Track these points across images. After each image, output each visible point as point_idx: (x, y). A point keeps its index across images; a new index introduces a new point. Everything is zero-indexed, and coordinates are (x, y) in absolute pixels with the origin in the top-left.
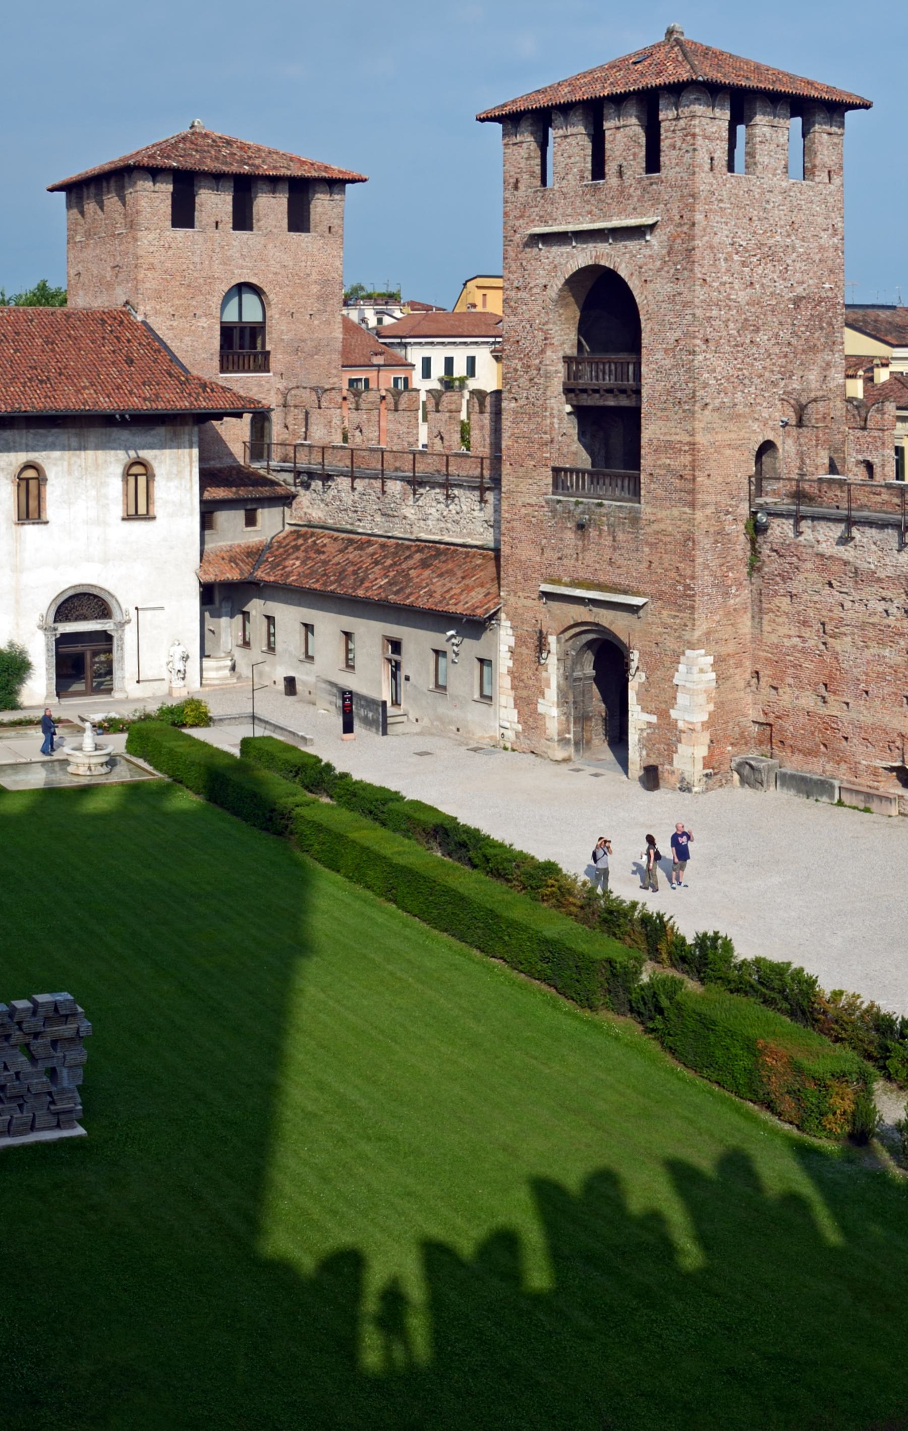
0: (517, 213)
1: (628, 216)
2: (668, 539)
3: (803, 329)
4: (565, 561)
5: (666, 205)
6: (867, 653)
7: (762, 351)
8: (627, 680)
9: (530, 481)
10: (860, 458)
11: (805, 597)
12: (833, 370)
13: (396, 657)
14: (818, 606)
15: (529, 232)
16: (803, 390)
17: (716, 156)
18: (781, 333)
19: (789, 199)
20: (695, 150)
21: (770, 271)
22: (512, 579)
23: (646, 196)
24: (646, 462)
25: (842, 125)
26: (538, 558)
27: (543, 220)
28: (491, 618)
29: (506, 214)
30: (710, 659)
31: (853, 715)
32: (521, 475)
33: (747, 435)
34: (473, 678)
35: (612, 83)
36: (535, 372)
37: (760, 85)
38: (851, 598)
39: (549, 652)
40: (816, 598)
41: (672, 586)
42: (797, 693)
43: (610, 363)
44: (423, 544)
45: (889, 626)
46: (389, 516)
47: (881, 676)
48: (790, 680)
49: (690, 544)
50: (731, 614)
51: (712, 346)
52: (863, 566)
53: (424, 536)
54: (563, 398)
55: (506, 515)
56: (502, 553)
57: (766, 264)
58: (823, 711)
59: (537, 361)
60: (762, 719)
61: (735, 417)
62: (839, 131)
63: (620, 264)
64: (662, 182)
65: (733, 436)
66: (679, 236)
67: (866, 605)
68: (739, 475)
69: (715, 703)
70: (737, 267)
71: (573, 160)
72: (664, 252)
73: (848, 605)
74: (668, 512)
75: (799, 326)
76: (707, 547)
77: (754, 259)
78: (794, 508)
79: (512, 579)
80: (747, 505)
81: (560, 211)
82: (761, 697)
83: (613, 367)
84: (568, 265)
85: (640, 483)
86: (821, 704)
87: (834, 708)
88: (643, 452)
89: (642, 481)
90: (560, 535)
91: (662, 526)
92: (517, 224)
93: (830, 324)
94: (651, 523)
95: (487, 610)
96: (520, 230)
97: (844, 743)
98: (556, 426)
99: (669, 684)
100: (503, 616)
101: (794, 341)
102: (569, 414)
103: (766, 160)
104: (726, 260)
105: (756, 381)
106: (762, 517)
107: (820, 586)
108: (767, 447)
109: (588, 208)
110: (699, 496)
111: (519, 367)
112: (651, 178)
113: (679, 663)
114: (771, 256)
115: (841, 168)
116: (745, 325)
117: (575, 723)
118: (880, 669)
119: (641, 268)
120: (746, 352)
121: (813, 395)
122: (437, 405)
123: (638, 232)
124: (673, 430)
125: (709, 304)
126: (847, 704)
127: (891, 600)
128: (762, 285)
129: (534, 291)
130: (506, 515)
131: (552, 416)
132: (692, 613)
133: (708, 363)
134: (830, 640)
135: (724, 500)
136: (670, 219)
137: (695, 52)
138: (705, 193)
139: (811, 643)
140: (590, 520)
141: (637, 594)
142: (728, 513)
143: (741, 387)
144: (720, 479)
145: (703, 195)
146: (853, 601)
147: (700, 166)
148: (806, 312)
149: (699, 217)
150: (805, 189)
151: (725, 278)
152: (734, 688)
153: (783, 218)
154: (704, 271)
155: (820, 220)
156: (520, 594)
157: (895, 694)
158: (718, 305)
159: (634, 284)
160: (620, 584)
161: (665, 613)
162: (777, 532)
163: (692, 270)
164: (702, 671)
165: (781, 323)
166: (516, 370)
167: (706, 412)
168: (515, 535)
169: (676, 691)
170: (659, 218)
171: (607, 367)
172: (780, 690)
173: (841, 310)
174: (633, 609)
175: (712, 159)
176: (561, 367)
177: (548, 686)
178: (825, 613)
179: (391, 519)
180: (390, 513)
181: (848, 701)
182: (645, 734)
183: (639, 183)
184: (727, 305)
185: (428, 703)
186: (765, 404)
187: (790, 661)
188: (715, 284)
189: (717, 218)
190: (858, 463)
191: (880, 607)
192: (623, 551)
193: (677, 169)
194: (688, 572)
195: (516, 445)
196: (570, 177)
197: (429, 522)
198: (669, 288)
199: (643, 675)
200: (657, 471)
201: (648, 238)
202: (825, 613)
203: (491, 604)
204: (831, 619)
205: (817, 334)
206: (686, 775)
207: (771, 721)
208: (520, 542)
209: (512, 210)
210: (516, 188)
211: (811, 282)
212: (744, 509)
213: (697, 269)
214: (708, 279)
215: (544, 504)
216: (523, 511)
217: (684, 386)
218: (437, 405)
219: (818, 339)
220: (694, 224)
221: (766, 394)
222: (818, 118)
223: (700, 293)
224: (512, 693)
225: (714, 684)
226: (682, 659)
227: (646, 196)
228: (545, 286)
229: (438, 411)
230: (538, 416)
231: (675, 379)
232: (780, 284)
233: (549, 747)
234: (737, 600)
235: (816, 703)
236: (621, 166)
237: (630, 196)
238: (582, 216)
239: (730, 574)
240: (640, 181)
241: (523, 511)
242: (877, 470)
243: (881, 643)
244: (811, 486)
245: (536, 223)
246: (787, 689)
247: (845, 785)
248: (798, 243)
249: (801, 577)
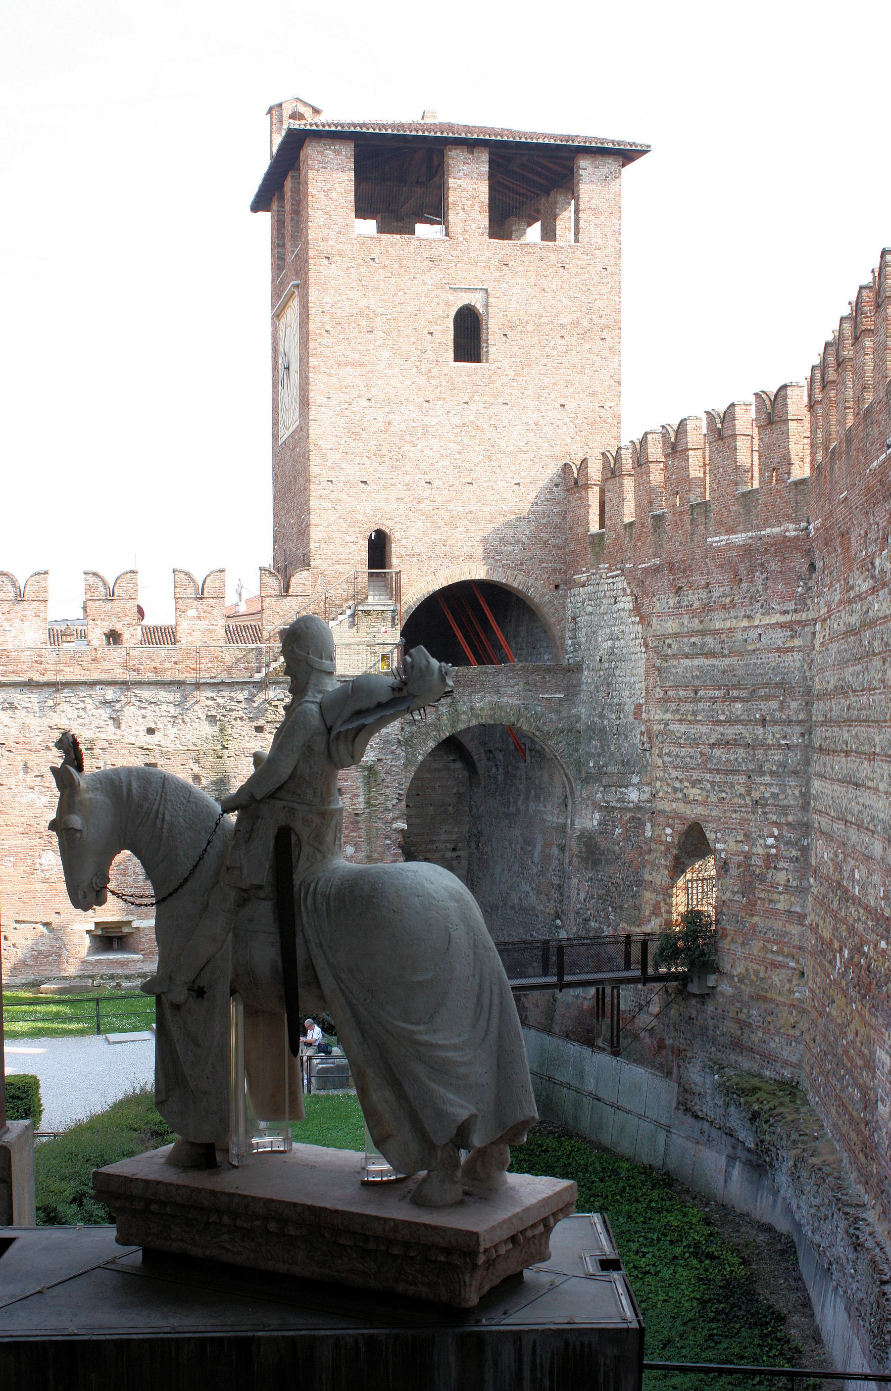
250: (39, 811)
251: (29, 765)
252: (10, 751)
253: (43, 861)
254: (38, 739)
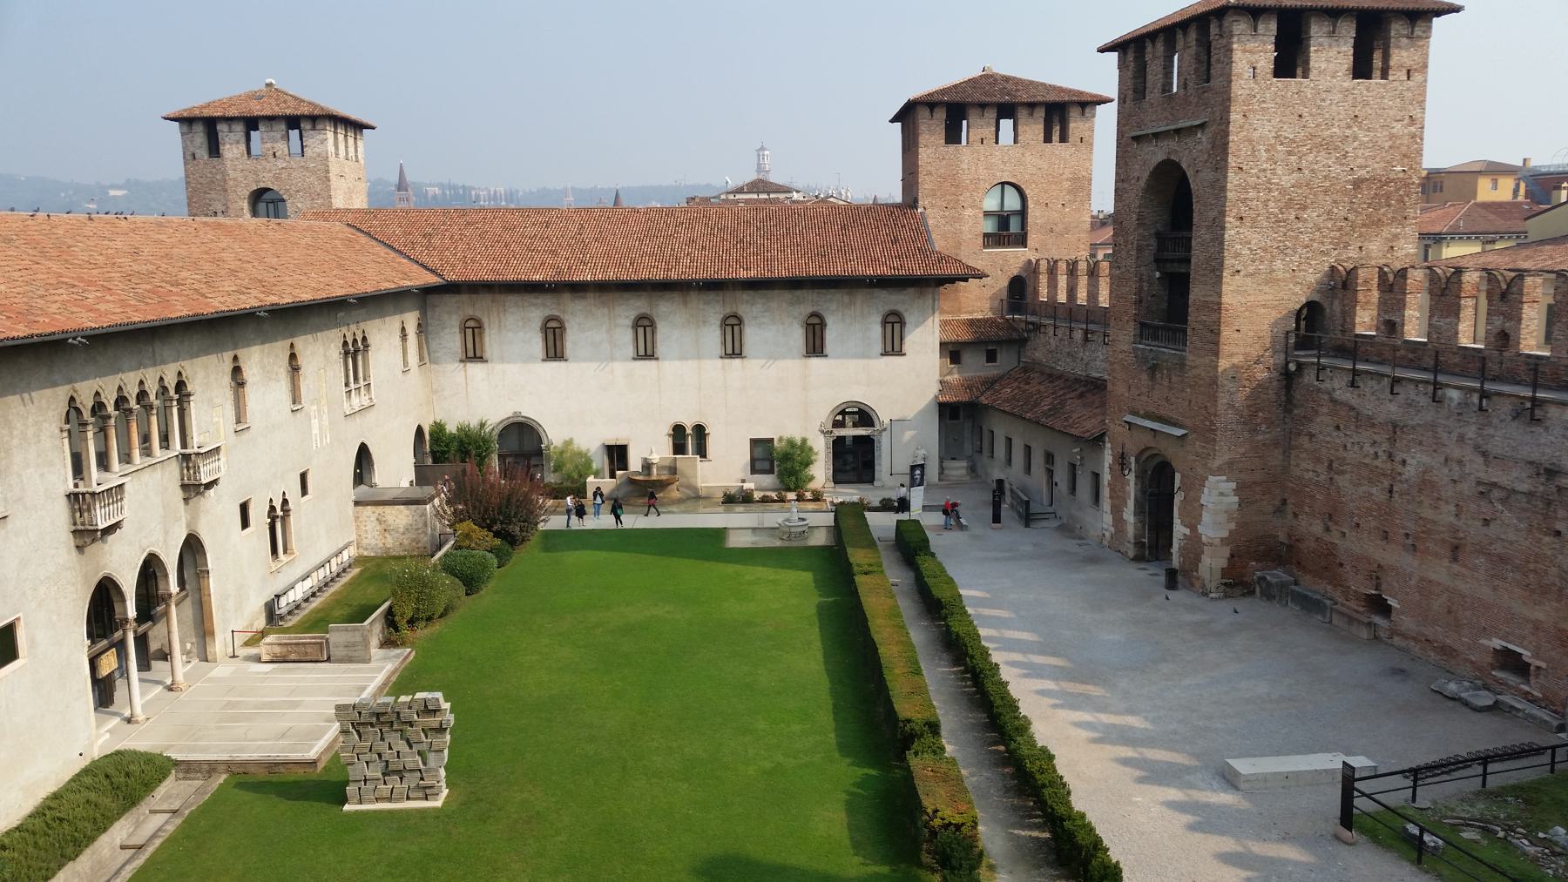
3: (1365, 206)
17: (1259, 65)
30: (1233, 485)
69: (1237, 523)
70: (1281, 156)
72: (1210, 146)
75: (1360, 204)
93: (1401, 201)
104: (1267, 151)
114: (1327, 146)
116: (1290, 203)
125: (1245, 188)
136: (1215, 120)
143: (1281, 256)
145: (1240, 99)
148: (1366, 193)
153: (1343, 112)
165: (1335, 202)
193: (1221, 79)
214: (1245, 167)
226: (1207, 483)
232: (1336, 169)
248: (1361, 134)
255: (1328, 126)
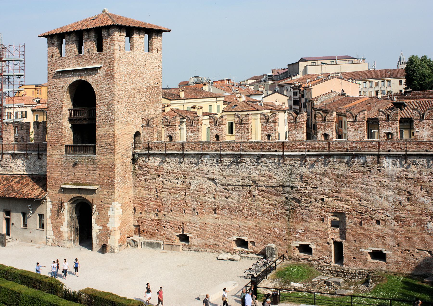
0: (52, 65)
1: (91, 65)
2: (105, 166)
3: (149, 96)
4: (70, 177)
5: (104, 61)
6: (171, 197)
7: (136, 104)
8: (92, 215)
9: (57, 150)
10: (168, 135)
11: (151, 181)
12: (158, 108)
13: (8, 217)
14: (155, 183)
15: (57, 70)
16: (149, 115)
17: (121, 46)
18: (142, 98)
19: (144, 58)
20: (114, 45)
21: (139, 80)
22: (51, 184)
23: (98, 58)
24: (98, 141)
25: (161, 36)
26: (60, 176)
27: (61, 66)
28: (43, 199)
29: (48, 65)
30: (120, 205)
31: (167, 218)
32: (54, 148)
33: (131, 130)
34: (37, 221)
35: (85, 26)
36: (59, 114)
37: (135, 26)
38: (166, 180)
39: (64, 209)
40: (154, 181)
41: (107, 181)
42: (148, 213)
43: (85, 110)
44: (17, 176)
45: (178, 187)
46: (4, 167)
47: (176, 204)
48: (146, 209)
49: (113, 167)
50: (126, 189)
51: (120, 102)
52: (169, 169)
53: (17, 173)
54: (69, 122)
55: (49, 163)
56: (47, 176)
57: (137, 77)
58: (157, 218)
59: (60, 111)
60: (137, 224)
61: (127, 125)
62: (160, 38)
63: (89, 79)
64: (103, 54)
65: (127, 131)
66: (109, 70)
67: (171, 181)
68: (129, 143)
69: (122, 220)
70: (128, 79)
71: (72, 48)
72: (104, 75)
73: (165, 182)
74: (106, 157)
75: (148, 95)
76: (119, 167)
77: (133, 76)
78: (147, 152)
79: (51, 184)
80: (131, 152)
81: (68, 64)
82: (136, 216)
83: (86, 111)
84: (71, 80)
85: (96, 148)
86: (156, 216)
87: (161, 217)
88: (97, 138)
89: (97, 147)
90: (68, 168)
91: (104, 162)
92: (52, 68)
94: (99, 161)
95: (42, 196)
96: (54, 70)
97: (164, 228)
98: (66, 131)
99: (107, 215)
100: (48, 198)
101: (146, 100)
102: (70, 127)
103: (137, 47)
104: (124, 77)
105: (134, 113)
106: (136, 156)
107: (155, 177)
108: (137, 134)
109: (77, 62)
110: (116, 151)
111: (53, 113)
112: (99, 53)
113: (110, 207)
114: (139, 75)
115: (161, 48)
117: (73, 233)
118: (175, 202)
119: (96, 80)
120: (131, 104)
121: (152, 117)
122: (22, 127)
123: (95, 70)
124: (107, 130)
125: (119, 90)
126: (165, 215)
127: (179, 179)
128: (136, 84)
129: (59, 89)
130: (49, 163)
131: (65, 128)
132: (114, 190)
133: (119, 108)
134: (159, 194)
135: (124, 151)
136: (106, 65)
137: (113, 17)
138: (118, 57)
139: (153, 196)
140: (78, 162)
141: (95, 185)
142: (125, 155)
143: (129, 115)
144: (123, 145)
145: (117, 58)
146: (166, 181)
147: (116, 49)
148: (150, 91)
149: (116, 64)
150: (150, 55)
151: (124, 82)
152: (128, 214)
153: (143, 63)
154: (117, 80)
155: (154, 64)
156: (54, 189)
157: (181, 210)
158: (122, 90)
159: (94, 85)
160: (89, 182)
161: (105, 191)
162: (141, 160)
163: (113, 80)
164: (117, 209)
165: (142, 95)
166: (52, 114)
167: (118, 124)
168: (52, 169)
169: (109, 217)
170: (102, 65)
171: (84, 111)
172: (143, 213)
173: (161, 90)
174: (93, 191)
175: (120, 47)
176: (68, 112)
177: (64, 221)
178: (157, 185)
179: (5, 168)
180: (5, 165)
181: (165, 214)
182: (98, 234)
183: (95, 55)
184: (125, 90)
185: (20, 233)
186: (137, 120)
187: (146, 203)
188: (121, 84)
189: (122, 65)
190: (167, 136)
191: (176, 181)
192: (90, 171)
193: (109, 50)
194: (113, 176)
195: (52, 139)
196: (71, 53)
197: (19, 168)
198: (106, 86)
199: (97, 213)
200: (102, 144)
201: (98, 71)
202: (157, 185)
203: (44, 194)
204: (159, 187)
205: (153, 98)
206: (112, 247)
207: (140, 223)
208: (54, 171)
209: (50, 64)
210: (52, 57)
211: (151, 82)
212: (130, 154)
213: (115, 80)
214: (119, 83)
215: (62, 158)
216: (55, 161)
217: (111, 116)
218: (22, 127)
219: (154, 99)
220: (114, 66)
221: (137, 117)
222: (154, 35)
223: (116, 87)
224: (51, 225)
225: (121, 213)
226: (111, 206)
227: (98, 58)
228: (62, 87)
229: (22, 129)
230: (60, 129)
231: (108, 114)
232: (142, 83)
233: (64, 243)
234: (128, 184)
235: (155, 216)
236: (89, 50)
237: (92, 59)
238: (75, 65)
239: (126, 176)
240: (96, 54)
241: (55, 161)
242: (174, 138)
243: (176, 193)
244: (152, 145)
245: (59, 68)
246: (145, 212)
247: (165, 243)
249: (149, 174)
250: (426, 206)
251: (423, 187)
252: (415, 181)
253: (428, 226)
254: (426, 177)
255: (139, 68)
